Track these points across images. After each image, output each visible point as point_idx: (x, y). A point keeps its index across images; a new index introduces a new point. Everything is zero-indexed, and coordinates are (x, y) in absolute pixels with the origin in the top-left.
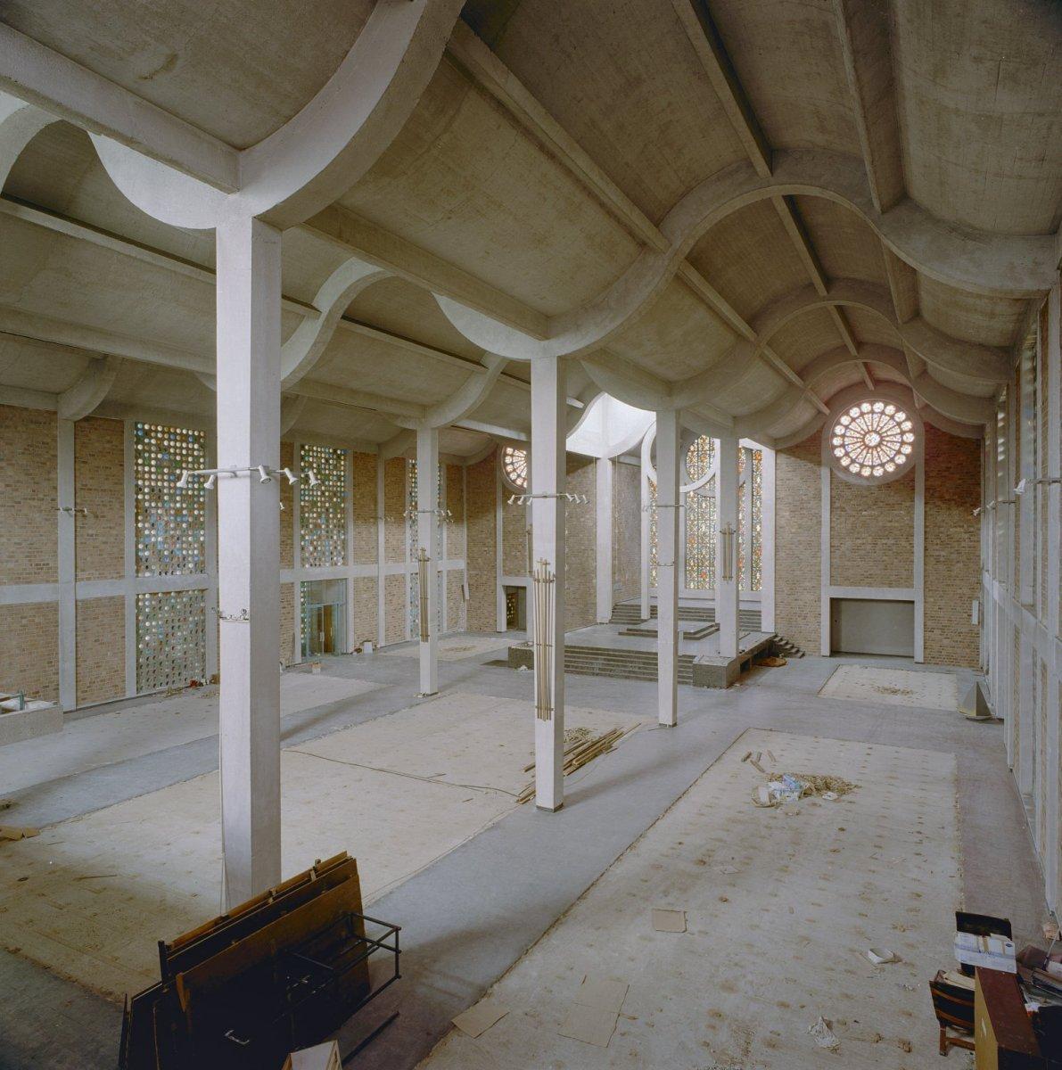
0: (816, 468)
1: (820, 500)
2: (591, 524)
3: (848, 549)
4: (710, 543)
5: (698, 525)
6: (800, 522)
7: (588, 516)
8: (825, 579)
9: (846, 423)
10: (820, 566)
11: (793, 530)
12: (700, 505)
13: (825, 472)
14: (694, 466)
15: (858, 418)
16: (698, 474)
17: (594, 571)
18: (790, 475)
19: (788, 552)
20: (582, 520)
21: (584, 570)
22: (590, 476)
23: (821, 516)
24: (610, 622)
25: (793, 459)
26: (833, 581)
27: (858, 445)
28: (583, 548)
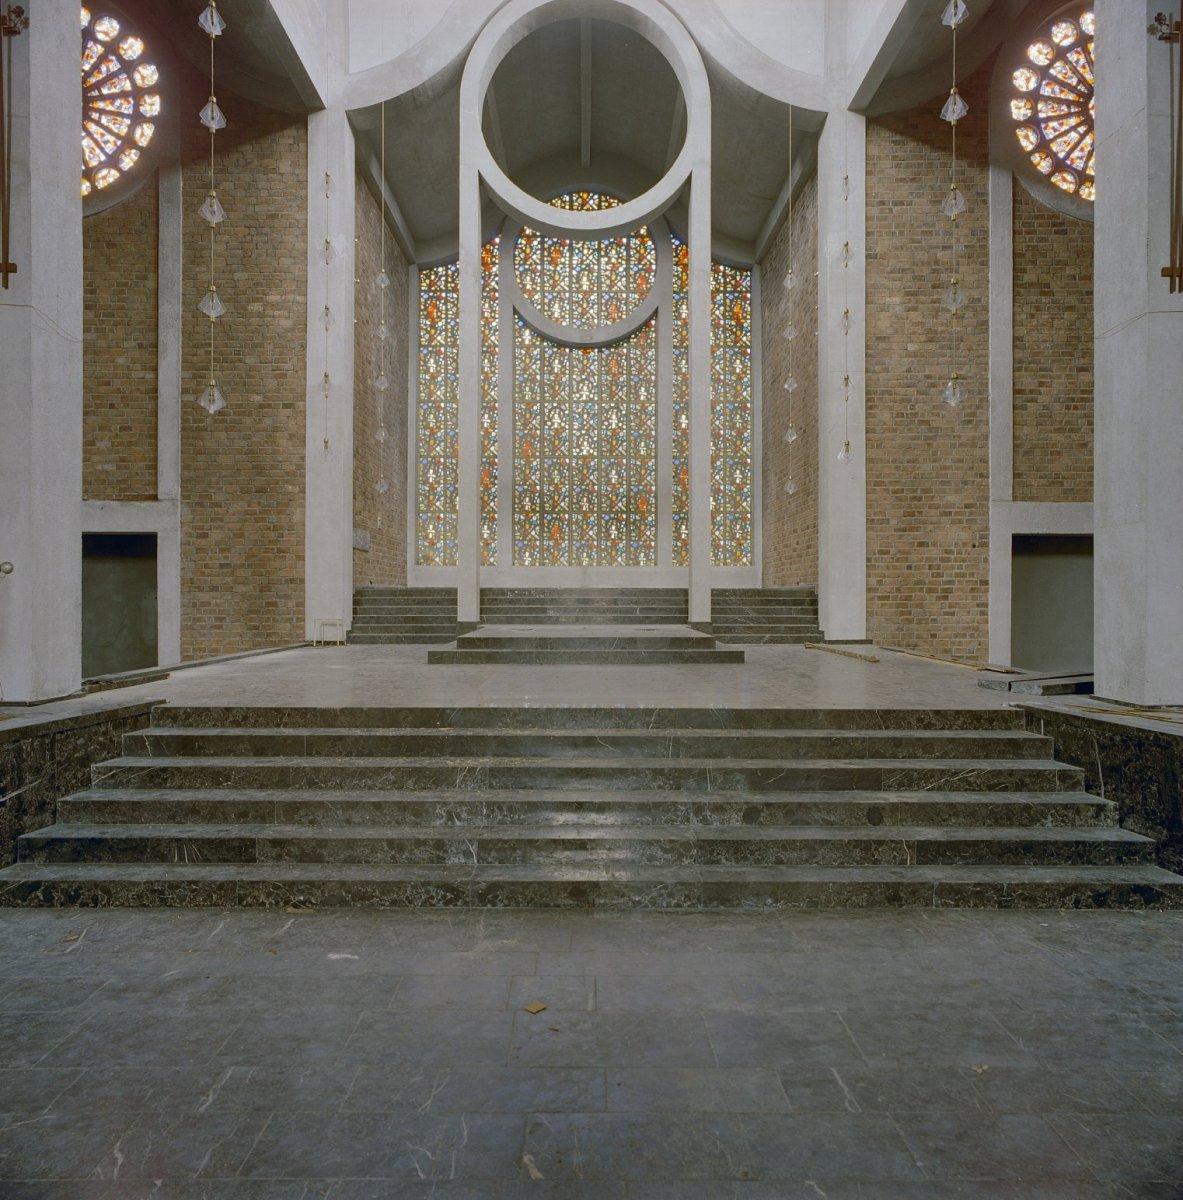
0: (973, 172)
1: (985, 264)
2: (286, 323)
3: (1057, 400)
4: (571, 457)
5: (542, 413)
6: (930, 323)
7: (273, 298)
8: (1000, 480)
9: (1042, 61)
10: (985, 446)
11: (911, 347)
12: (545, 363)
13: (997, 185)
14: (534, 271)
15: (1070, 48)
16: (543, 291)
17: (298, 474)
18: (904, 191)
19: (898, 407)
20: (256, 307)
21: (259, 470)
22: (285, 167)
23: (986, 309)
24: (351, 639)
25: (912, 145)
26: (1021, 491)
27: (1073, 121)
28: (258, 399)
